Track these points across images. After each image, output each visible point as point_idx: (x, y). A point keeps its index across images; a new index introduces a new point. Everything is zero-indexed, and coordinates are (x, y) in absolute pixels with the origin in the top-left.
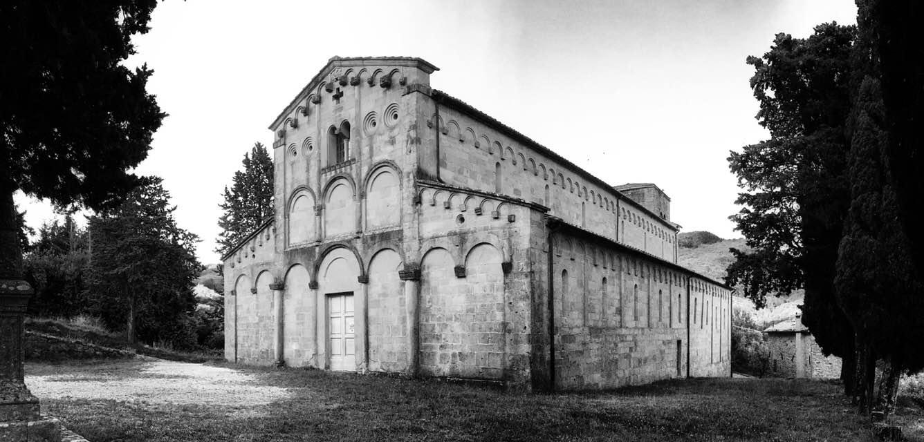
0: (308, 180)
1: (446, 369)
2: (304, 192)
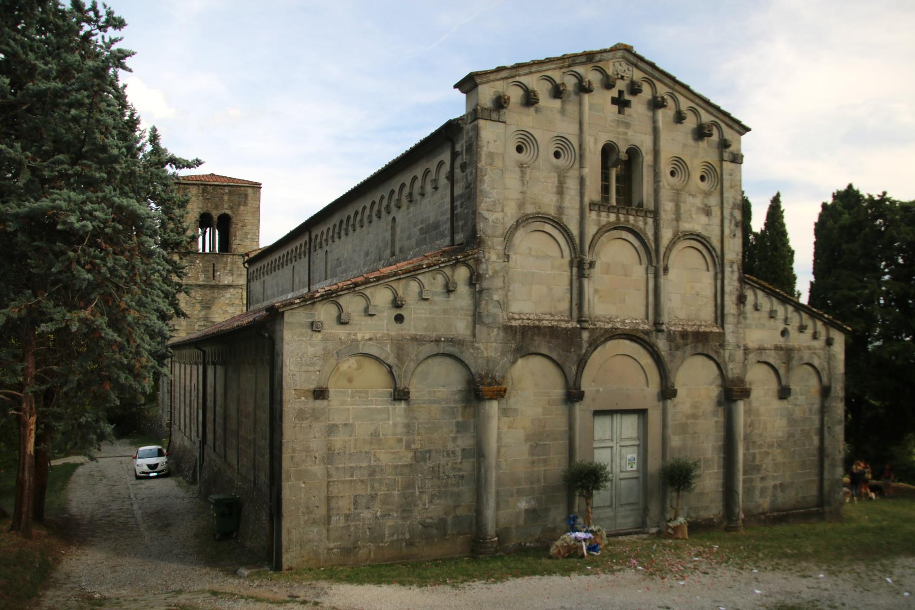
0: (560, 209)
1: (765, 503)
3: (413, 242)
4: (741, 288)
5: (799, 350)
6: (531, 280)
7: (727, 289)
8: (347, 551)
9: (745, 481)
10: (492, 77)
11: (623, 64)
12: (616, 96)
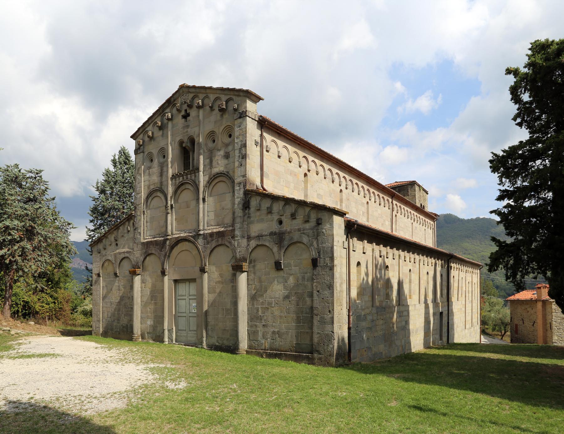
2: (159, 194)
4: (246, 198)
5: (290, 233)
10: (138, 134)
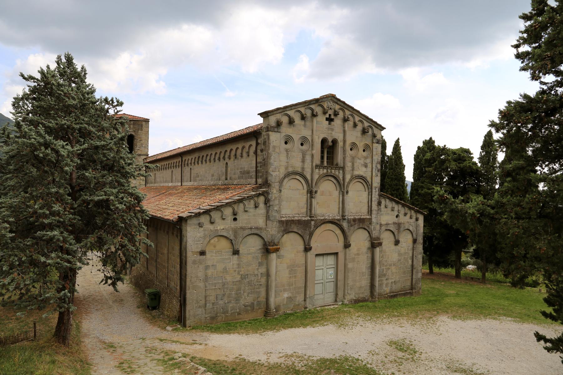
0: (303, 169)
1: (387, 290)
3: (237, 176)
6: (291, 201)
7: (373, 199)
8: (213, 318)
9: (379, 281)
10: (275, 112)
11: (331, 102)
12: (328, 117)
